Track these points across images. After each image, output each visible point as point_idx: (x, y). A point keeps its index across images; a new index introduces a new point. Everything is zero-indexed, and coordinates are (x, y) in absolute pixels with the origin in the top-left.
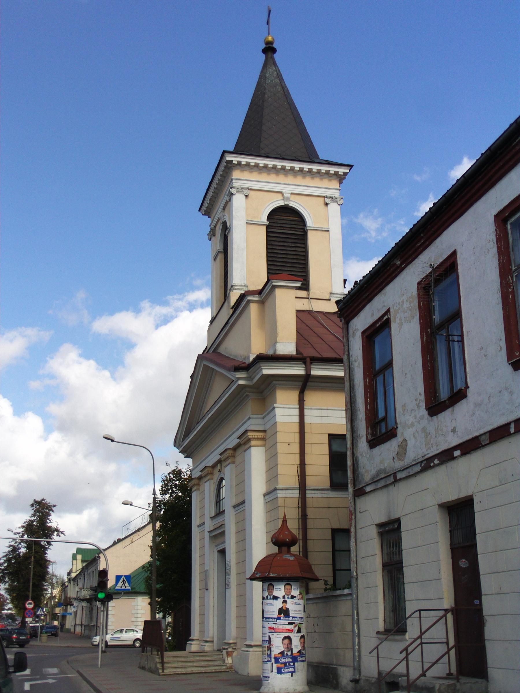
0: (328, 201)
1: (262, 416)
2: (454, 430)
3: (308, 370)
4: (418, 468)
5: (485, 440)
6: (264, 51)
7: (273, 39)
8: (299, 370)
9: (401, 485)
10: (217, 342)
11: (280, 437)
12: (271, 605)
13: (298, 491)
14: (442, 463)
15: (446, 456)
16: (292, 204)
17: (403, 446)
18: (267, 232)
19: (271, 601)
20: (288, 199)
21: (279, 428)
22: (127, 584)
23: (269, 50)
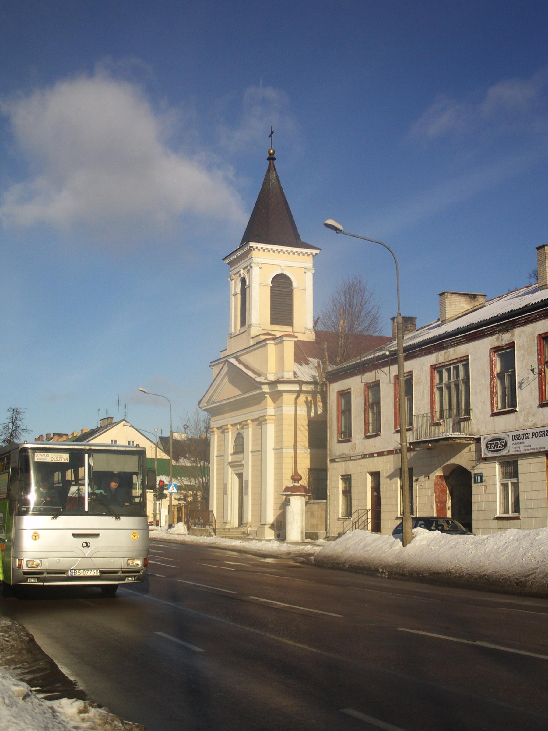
0: (306, 271)
2: (375, 446)
3: (301, 388)
4: (360, 457)
5: (385, 453)
6: (269, 159)
7: (274, 152)
8: (296, 387)
9: (351, 462)
10: (239, 354)
11: (285, 422)
14: (369, 457)
15: (371, 455)
16: (286, 273)
17: (354, 446)
18: (271, 290)
20: (284, 270)
21: (284, 417)
22: (175, 489)
23: (271, 158)
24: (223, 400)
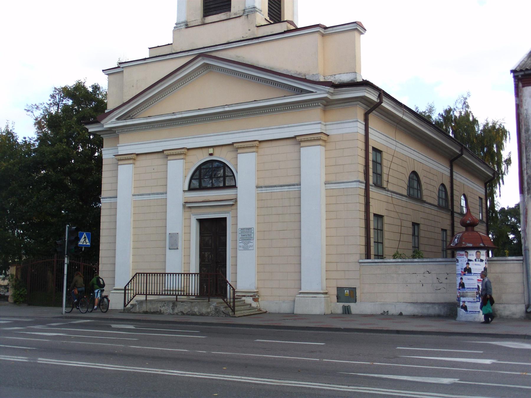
1: (325, 123)
12: (479, 265)
13: (364, 185)
19: (479, 263)
24: (181, 112)
